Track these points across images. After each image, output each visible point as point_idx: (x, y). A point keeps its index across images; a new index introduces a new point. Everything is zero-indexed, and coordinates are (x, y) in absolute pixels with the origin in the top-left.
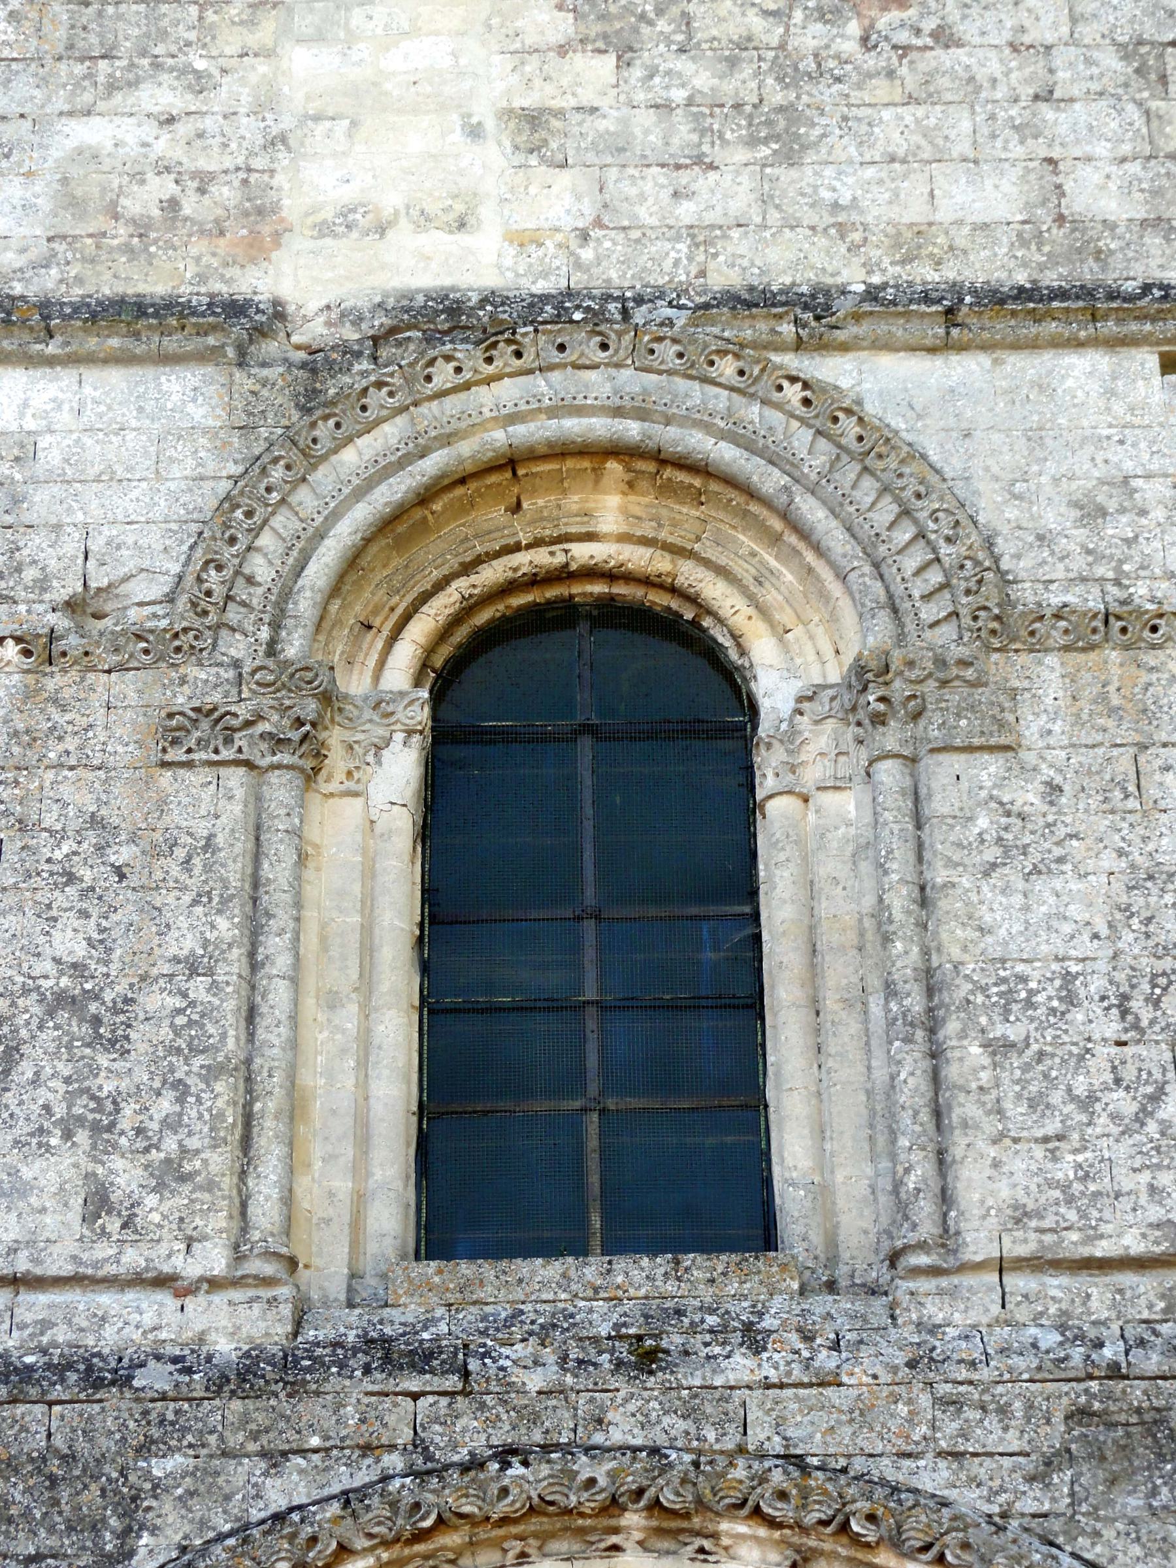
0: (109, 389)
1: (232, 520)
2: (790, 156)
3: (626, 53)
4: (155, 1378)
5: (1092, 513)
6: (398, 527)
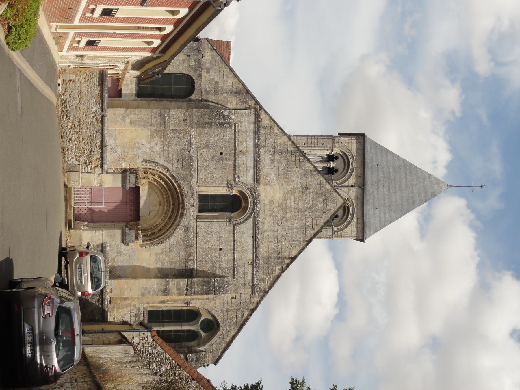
2: (269, 216)
4: (192, 182)
5: (242, 232)
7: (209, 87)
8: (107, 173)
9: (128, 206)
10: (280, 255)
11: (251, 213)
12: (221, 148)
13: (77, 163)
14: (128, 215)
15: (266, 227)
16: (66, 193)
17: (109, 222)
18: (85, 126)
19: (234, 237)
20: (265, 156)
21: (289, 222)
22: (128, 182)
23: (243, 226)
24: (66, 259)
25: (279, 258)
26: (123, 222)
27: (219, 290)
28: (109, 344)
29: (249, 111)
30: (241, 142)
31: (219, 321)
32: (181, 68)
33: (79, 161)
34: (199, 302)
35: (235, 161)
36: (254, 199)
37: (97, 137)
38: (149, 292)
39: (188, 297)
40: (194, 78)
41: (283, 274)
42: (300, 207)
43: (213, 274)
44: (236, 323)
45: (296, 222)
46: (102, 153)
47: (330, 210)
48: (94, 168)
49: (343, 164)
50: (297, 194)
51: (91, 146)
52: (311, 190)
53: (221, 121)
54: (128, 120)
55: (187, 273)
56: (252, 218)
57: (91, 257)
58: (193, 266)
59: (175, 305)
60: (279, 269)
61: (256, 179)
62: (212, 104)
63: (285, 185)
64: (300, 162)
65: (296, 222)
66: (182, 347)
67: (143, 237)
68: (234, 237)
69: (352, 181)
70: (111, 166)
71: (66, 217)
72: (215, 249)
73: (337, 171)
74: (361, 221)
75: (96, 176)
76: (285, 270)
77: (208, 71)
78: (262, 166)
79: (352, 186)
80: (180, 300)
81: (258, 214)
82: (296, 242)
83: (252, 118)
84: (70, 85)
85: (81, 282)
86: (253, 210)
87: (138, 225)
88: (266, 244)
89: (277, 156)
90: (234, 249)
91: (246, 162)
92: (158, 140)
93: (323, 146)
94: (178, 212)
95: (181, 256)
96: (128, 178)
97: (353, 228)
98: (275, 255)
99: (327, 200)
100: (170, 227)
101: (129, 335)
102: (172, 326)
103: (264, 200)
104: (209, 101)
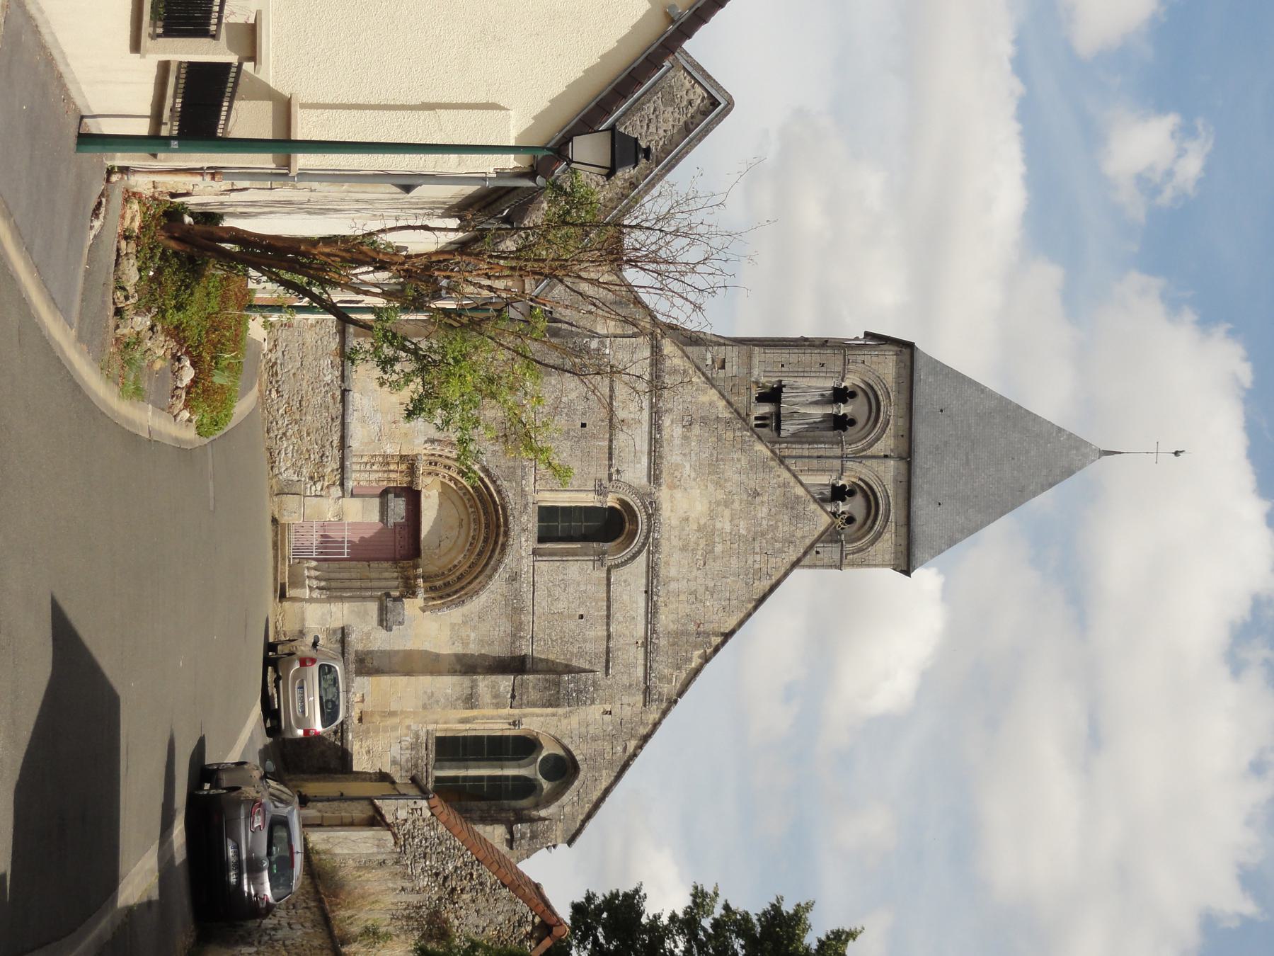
0: (645, 471)
8: (352, 495)
10: (702, 629)
11: (644, 545)
13: (296, 478)
14: (397, 559)
15: (673, 572)
16: (276, 535)
18: (311, 410)
19: (608, 591)
20: (672, 429)
21: (719, 562)
22: (390, 513)
23: (626, 569)
24: (276, 671)
25: (698, 634)
26: (387, 560)
27: (578, 698)
28: (351, 824)
29: (641, 339)
31: (578, 758)
33: (300, 474)
34: (536, 721)
35: (611, 441)
36: (649, 517)
37: (334, 429)
38: (437, 702)
39: (516, 711)
41: (708, 667)
42: (743, 532)
43: (567, 666)
44: (611, 763)
45: (734, 561)
46: (343, 460)
47: (803, 537)
48: (328, 487)
49: (866, 408)
50: (736, 506)
51: (323, 446)
52: (765, 499)
55: (515, 665)
56: (645, 553)
57: (321, 667)
58: (526, 650)
59: (491, 726)
60: (700, 657)
61: (654, 476)
62: (565, 326)
63: (711, 487)
64: (743, 442)
65: (734, 561)
66: (502, 810)
67: (426, 591)
68: (608, 591)
69: (886, 444)
71: (276, 579)
72: (570, 617)
73: (852, 422)
74: (903, 530)
75: (331, 501)
78: (666, 449)
79: (886, 456)
80: (500, 717)
81: (657, 545)
82: (734, 602)
84: (284, 334)
85: (303, 712)
86: (647, 538)
87: (416, 567)
89: (696, 429)
90: (608, 617)
91: (634, 441)
93: (823, 369)
94: (496, 542)
95: (502, 629)
96: (391, 505)
97: (888, 543)
98: (692, 628)
99: (797, 517)
100: (481, 572)
101: (388, 808)
102: (484, 767)
104: (560, 321)
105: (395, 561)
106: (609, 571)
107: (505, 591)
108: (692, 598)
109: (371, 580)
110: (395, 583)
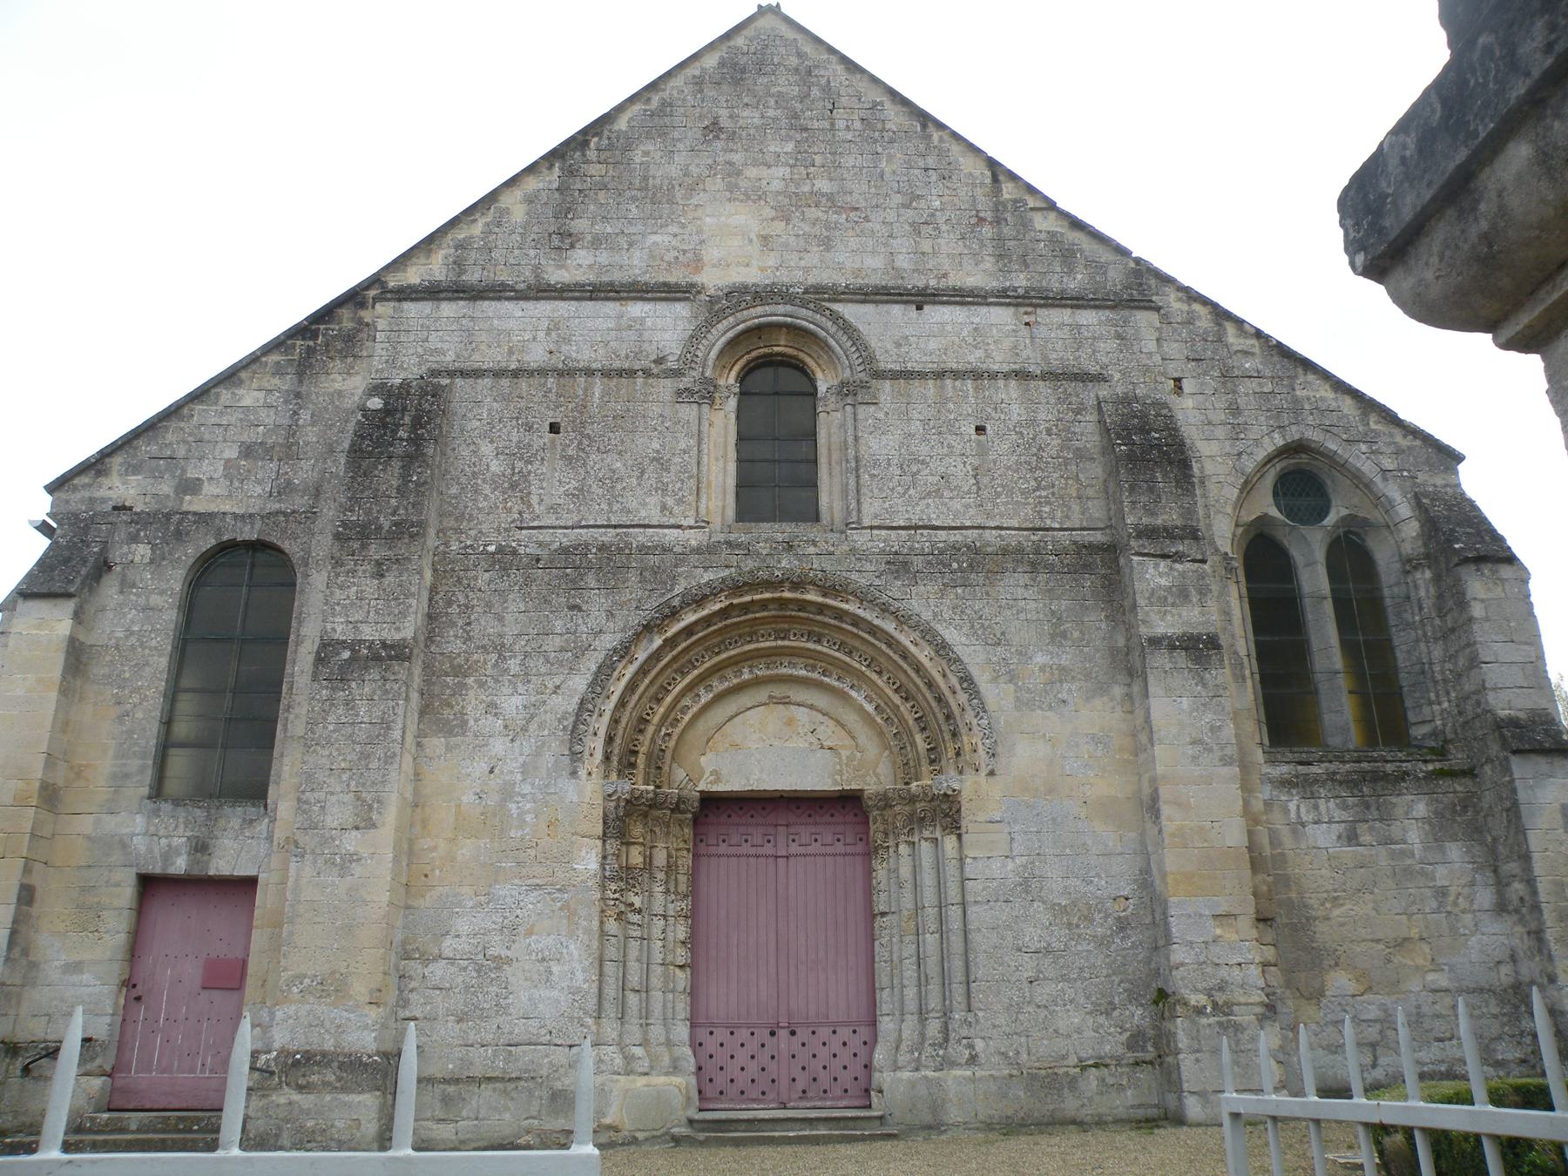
0: (661, 307)
1: (694, 338)
2: (828, 250)
3: (788, 221)
4: (678, 549)
5: (898, 345)
6: (732, 344)
7: (259, 482)
9: (794, 848)
10: (989, 215)
12: (529, 428)
17: (871, 939)
19: (922, 375)
21: (849, 185)
26: (869, 872)
30: (511, 352)
31: (1280, 442)
32: (156, 600)
40: (212, 542)
42: (790, 147)
47: (799, 55)
50: (736, 158)
53: (407, 419)
54: (351, 842)
65: (849, 161)
68: (922, 375)
70: (588, 931)
72: (982, 451)
76: (1046, 198)
77: (190, 487)
78: (617, 277)
81: (818, 290)
82: (931, 161)
83: (414, 310)
88: (946, 265)
89: (579, 225)
90: (977, 375)
91: (594, 331)
92: (472, 703)
94: (821, 609)
95: (1020, 592)
103: (762, 269)
105: (870, 854)
106: (879, 375)
107: (932, 588)
108: (925, 229)
109: (918, 908)
110: (925, 847)
